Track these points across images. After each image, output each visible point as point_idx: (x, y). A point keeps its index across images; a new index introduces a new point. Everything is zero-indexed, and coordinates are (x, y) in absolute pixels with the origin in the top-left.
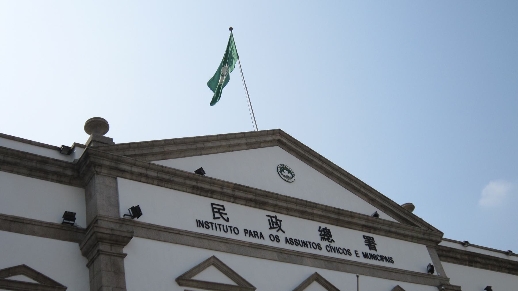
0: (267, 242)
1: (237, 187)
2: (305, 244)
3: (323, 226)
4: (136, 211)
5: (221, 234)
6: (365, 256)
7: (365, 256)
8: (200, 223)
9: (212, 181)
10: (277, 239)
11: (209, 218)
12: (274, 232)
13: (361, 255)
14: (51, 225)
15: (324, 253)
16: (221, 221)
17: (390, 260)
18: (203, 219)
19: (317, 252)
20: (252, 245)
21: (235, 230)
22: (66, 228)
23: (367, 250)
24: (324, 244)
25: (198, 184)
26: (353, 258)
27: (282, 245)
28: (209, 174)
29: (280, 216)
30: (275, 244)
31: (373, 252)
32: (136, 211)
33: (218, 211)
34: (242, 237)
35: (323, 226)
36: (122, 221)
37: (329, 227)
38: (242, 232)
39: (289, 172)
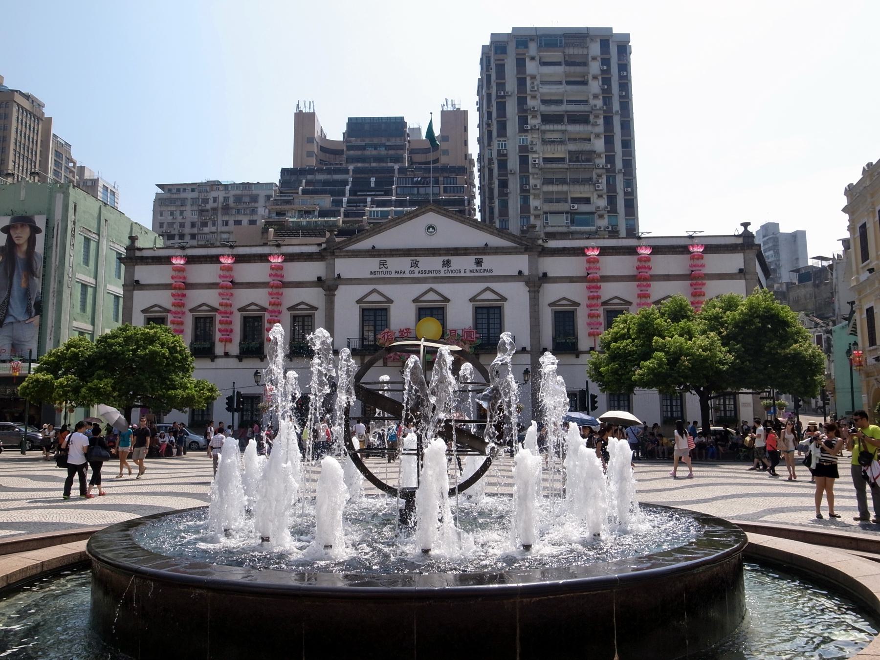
0: (407, 275)
1: (391, 250)
2: (430, 272)
3: (446, 258)
4: (339, 275)
5: (383, 276)
6: (471, 271)
7: (471, 271)
8: (372, 273)
9: (379, 250)
10: (413, 272)
11: (377, 269)
12: (413, 269)
13: (468, 272)
14: (313, 282)
15: (442, 274)
16: (384, 269)
17: (491, 271)
18: (373, 270)
19: (438, 275)
20: (397, 278)
21: (390, 272)
22: (320, 282)
23: (475, 267)
24: (443, 270)
25: (373, 253)
26: (463, 274)
27: (416, 275)
28: (378, 247)
29: (418, 259)
30: (412, 276)
31: (479, 268)
32: (339, 275)
33: (383, 264)
34: (393, 275)
35: (446, 258)
36: (335, 280)
37: (450, 258)
38: (393, 272)
39: (433, 228)
